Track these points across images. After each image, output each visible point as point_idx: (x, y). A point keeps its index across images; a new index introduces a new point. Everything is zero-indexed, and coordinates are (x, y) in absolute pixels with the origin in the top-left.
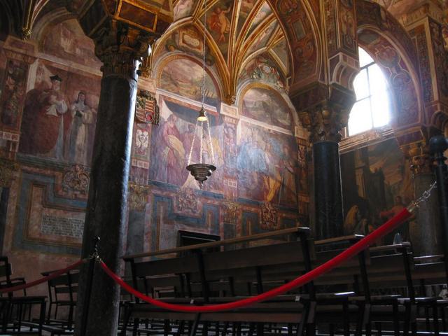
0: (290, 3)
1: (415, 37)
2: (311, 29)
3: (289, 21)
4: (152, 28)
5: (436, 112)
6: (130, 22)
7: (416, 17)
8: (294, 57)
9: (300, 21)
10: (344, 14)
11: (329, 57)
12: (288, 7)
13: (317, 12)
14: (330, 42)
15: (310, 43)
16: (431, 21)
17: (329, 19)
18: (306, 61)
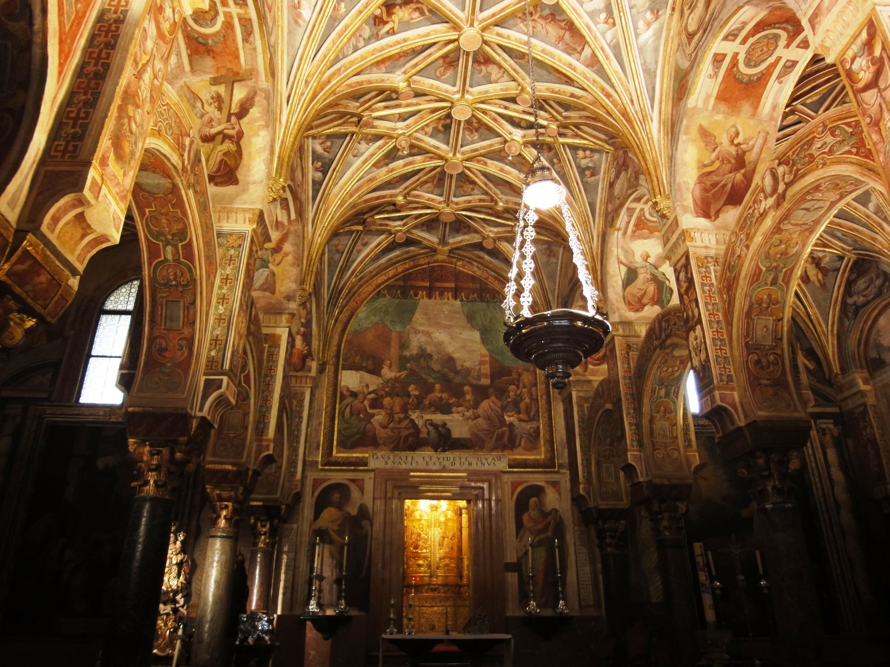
0: (179, 273)
1: (266, 346)
2: (194, 323)
3: (164, 295)
4: (45, 307)
5: (266, 453)
6: (18, 290)
7: (275, 322)
8: (149, 348)
9: (182, 304)
10: (240, 320)
11: (205, 374)
12: (172, 278)
13: (209, 304)
14: (213, 353)
15: (184, 343)
16: (290, 334)
17: (220, 319)
18: (169, 364)
